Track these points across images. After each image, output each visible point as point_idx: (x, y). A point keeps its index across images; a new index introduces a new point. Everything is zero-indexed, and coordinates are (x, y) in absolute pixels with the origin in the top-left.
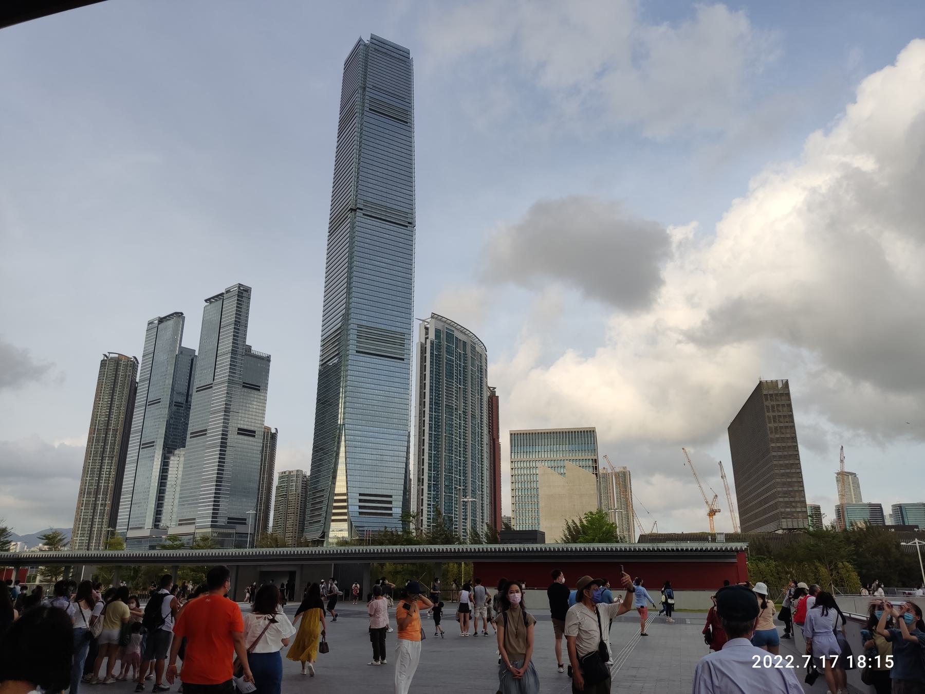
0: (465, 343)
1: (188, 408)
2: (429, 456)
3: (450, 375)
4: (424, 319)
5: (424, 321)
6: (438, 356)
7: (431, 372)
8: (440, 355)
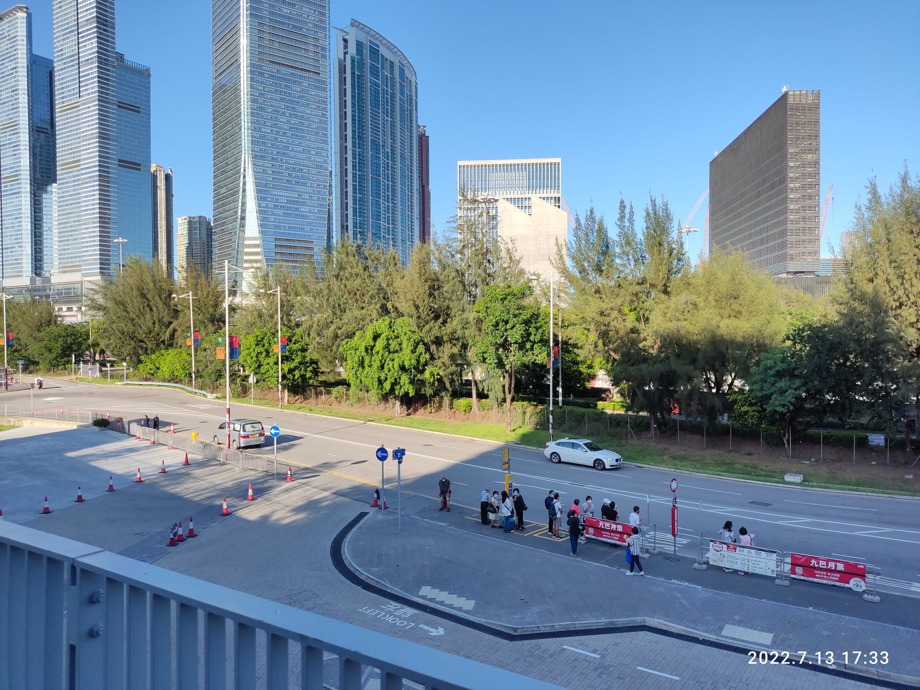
0: (392, 63)
2: (352, 130)
3: (376, 104)
7: (353, 97)
8: (363, 76)
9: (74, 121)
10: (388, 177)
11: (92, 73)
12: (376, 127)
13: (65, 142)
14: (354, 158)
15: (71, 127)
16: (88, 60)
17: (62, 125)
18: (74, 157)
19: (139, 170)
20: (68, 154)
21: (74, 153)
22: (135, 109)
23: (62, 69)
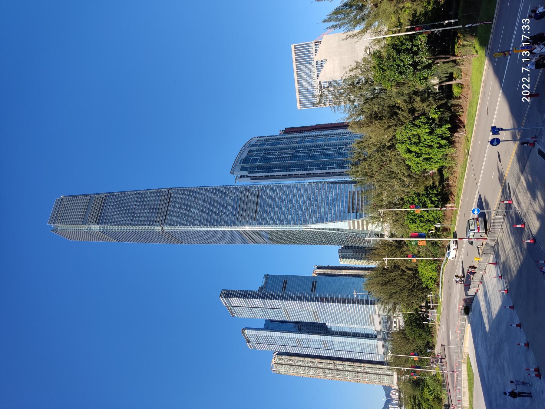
0: (250, 151)
1: (301, 323)
3: (271, 159)
4: (235, 179)
5: (236, 179)
6: (258, 168)
7: (268, 172)
8: (258, 167)
9: (294, 313)
10: (309, 150)
11: (270, 302)
12: (283, 158)
13: (304, 318)
14: (300, 170)
15: (296, 314)
16: (264, 304)
17: (296, 318)
18: (312, 314)
19: (316, 282)
20: (311, 317)
21: (310, 314)
22: (285, 283)
23: (269, 316)
